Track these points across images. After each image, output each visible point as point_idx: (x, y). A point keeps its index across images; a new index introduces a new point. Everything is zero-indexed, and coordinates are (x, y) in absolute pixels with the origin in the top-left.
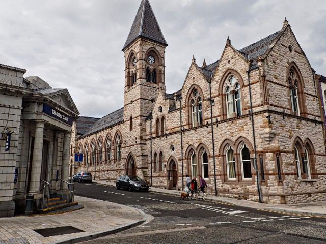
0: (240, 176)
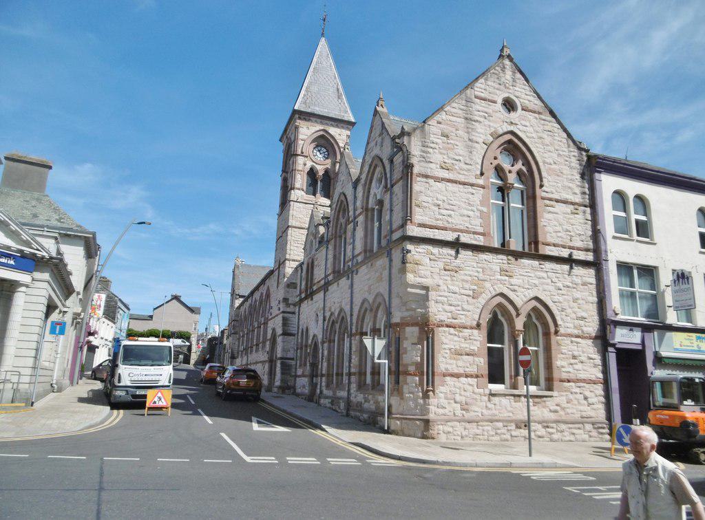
0: (340, 377)
